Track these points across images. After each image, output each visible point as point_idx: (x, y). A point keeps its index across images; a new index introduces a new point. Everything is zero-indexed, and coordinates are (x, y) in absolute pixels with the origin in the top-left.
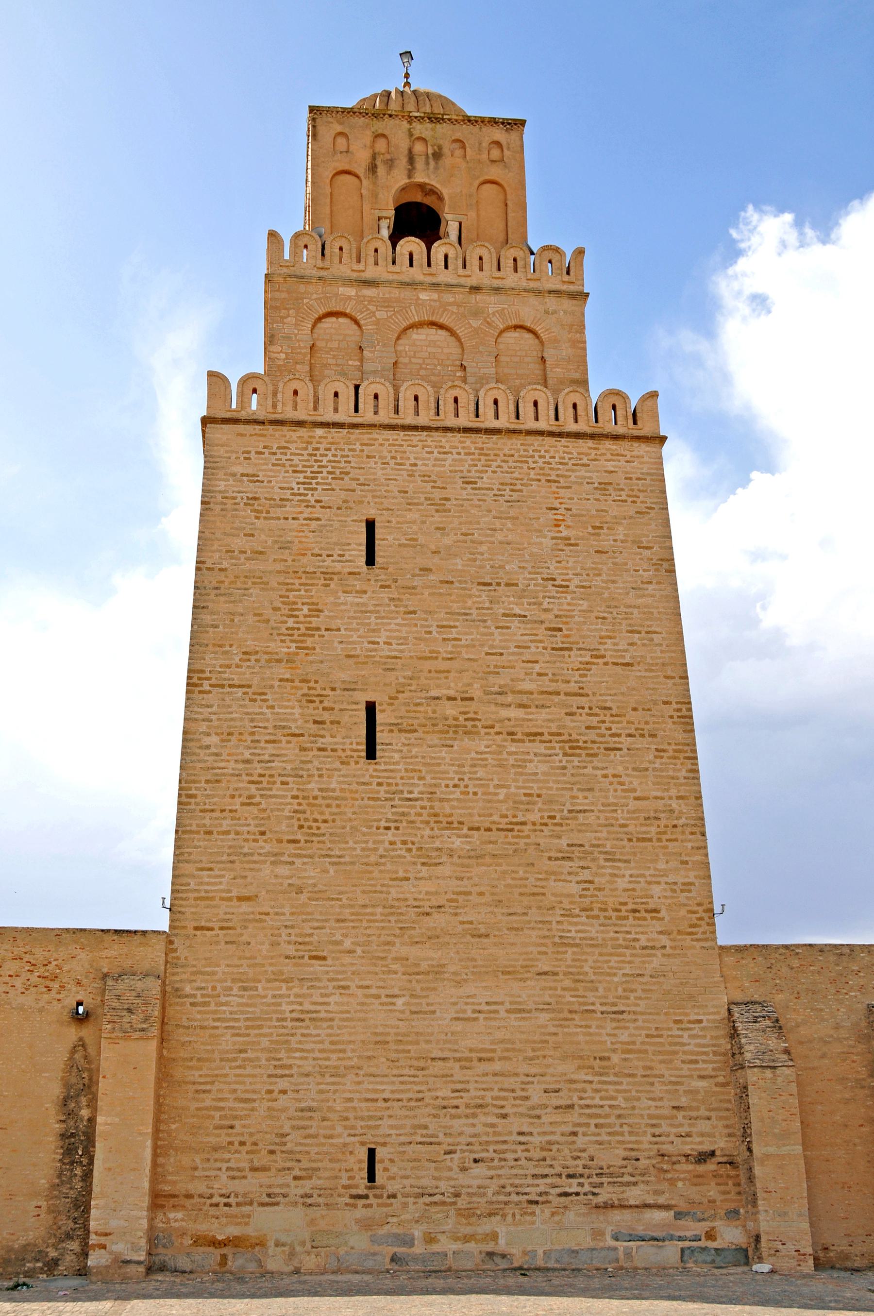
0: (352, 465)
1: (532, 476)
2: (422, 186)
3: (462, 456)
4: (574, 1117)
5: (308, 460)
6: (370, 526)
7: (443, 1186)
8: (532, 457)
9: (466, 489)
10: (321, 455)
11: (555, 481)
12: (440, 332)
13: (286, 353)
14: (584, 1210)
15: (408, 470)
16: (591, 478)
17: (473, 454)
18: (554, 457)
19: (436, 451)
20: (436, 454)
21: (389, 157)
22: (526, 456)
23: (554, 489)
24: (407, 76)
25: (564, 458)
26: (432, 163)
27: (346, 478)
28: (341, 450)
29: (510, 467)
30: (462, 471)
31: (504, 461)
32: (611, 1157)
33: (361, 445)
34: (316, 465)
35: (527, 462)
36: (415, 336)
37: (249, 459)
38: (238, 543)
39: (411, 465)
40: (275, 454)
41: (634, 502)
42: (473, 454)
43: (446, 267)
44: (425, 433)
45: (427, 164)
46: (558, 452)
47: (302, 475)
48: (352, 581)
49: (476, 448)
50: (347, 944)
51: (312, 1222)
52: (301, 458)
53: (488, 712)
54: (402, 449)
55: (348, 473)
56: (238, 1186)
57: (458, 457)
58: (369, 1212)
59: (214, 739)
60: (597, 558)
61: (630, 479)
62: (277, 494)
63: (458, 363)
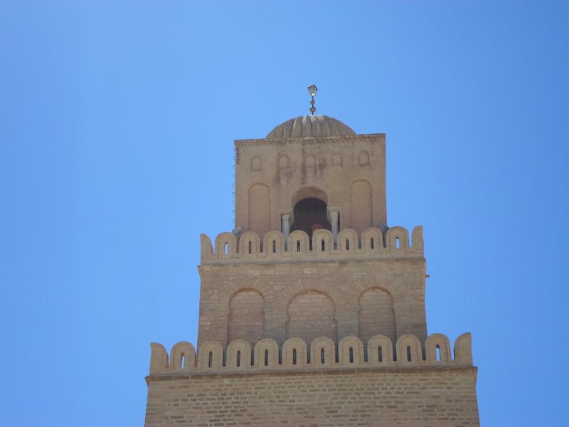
0: (249, 404)
1: (377, 404)
2: (312, 189)
3: (327, 392)
5: (218, 403)
8: (378, 389)
9: (329, 417)
10: (228, 399)
11: (394, 407)
12: (320, 296)
13: (212, 321)
15: (287, 406)
16: (421, 403)
17: (334, 390)
18: (393, 388)
19: (308, 390)
20: (308, 392)
21: (288, 170)
22: (373, 389)
23: (393, 413)
24: (313, 102)
25: (401, 388)
26: (318, 172)
27: (244, 414)
28: (241, 394)
29: (361, 398)
30: (326, 403)
31: (356, 394)
33: (256, 388)
34: (223, 406)
35: (373, 393)
36: (302, 301)
37: (177, 405)
39: (290, 401)
40: (195, 400)
41: (453, 419)
42: (334, 390)
43: (323, 249)
44: (301, 377)
45: (315, 172)
46: (396, 384)
47: (213, 415)
49: (336, 385)
52: (213, 401)
54: (284, 390)
55: (245, 411)
57: (323, 393)
61: (450, 401)
63: (332, 318)
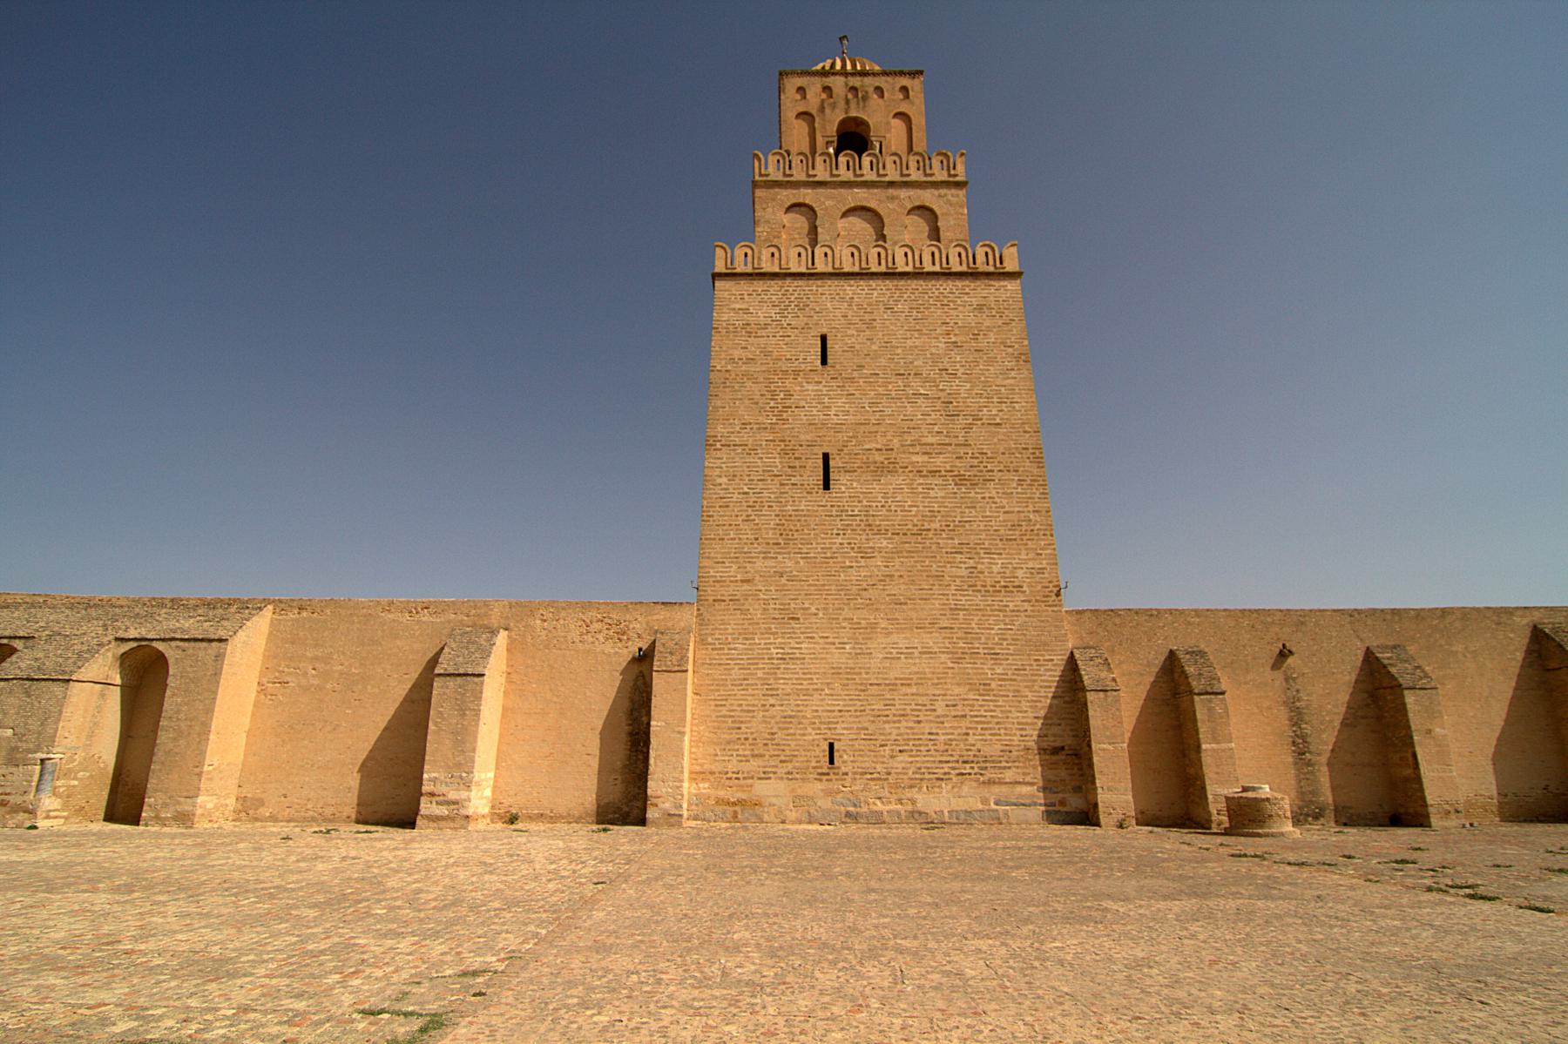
2: (855, 119)
4: (965, 723)
6: (824, 339)
7: (879, 767)
14: (974, 784)
32: (992, 750)
38: (737, 353)
48: (812, 375)
50: (813, 610)
51: (793, 790)
53: (903, 459)
56: (745, 767)
58: (830, 785)
59: (724, 480)
60: (976, 355)
62: (762, 321)
